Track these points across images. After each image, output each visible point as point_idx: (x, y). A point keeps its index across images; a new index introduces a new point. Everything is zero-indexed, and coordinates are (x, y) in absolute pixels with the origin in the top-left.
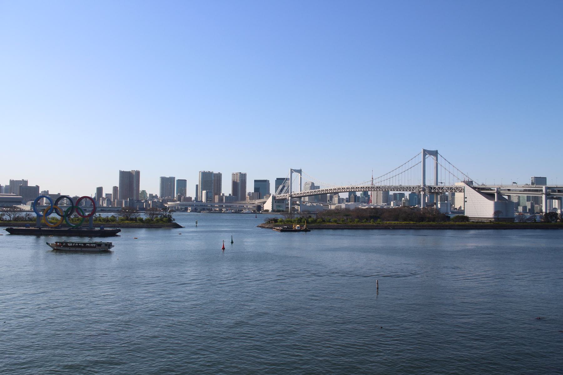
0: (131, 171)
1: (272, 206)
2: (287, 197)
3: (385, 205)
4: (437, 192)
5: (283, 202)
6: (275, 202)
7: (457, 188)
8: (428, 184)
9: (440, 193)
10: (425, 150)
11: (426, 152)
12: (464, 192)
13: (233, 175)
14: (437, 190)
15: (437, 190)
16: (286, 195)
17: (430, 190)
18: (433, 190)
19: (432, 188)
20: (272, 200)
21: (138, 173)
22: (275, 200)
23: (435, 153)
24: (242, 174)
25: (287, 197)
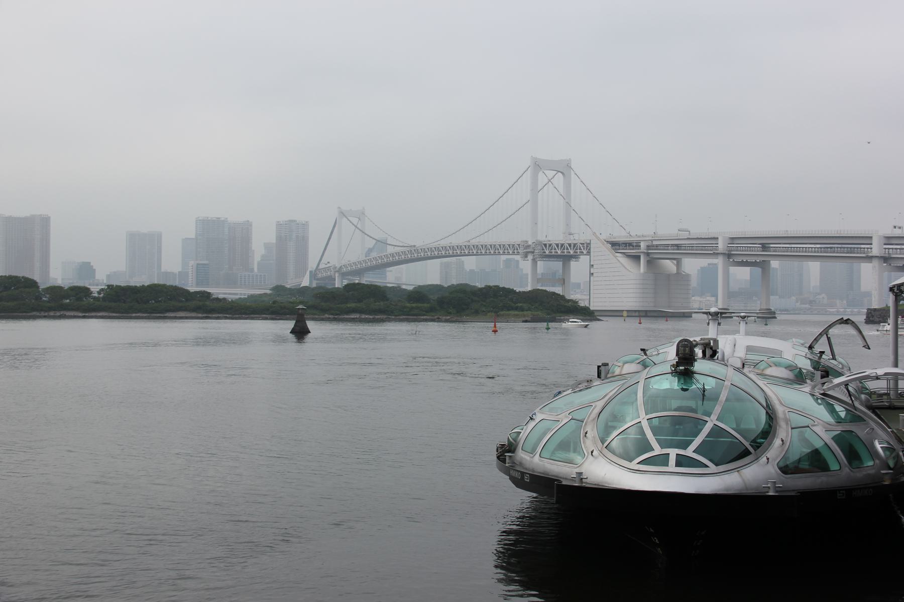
0: (28, 215)
7: (584, 244)
8: (542, 238)
10: (536, 158)
11: (538, 166)
13: (279, 225)
19: (545, 245)
20: (309, 281)
21: (45, 221)
22: (318, 279)
23: (564, 169)
24: (298, 224)
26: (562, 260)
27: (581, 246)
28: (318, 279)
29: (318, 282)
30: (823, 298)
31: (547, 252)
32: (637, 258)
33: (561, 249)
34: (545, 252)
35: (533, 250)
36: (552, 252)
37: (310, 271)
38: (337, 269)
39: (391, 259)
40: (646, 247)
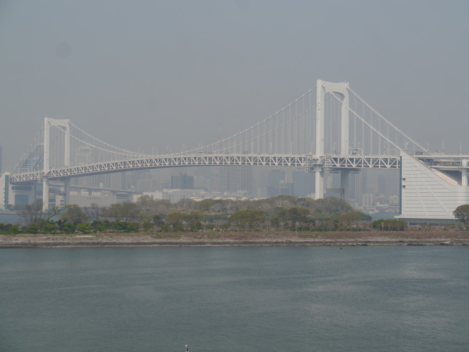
1: (6, 197)
2: (39, 177)
3: (245, 194)
4: (346, 167)
5: (30, 189)
6: (13, 188)
9: (354, 169)
12: (400, 167)
14: (346, 164)
15: (346, 164)
16: (37, 174)
17: (333, 163)
18: (340, 163)
19: (336, 159)
20: (4, 185)
25: (39, 177)
26: (340, 171)
27: (382, 160)
28: (13, 184)
29: (13, 186)
30: (395, 198)
31: (338, 165)
32: (456, 175)
33: (356, 163)
34: (336, 166)
35: (321, 163)
36: (345, 166)
37: (6, 176)
38: (45, 175)
39: (123, 167)
40: (467, 164)
